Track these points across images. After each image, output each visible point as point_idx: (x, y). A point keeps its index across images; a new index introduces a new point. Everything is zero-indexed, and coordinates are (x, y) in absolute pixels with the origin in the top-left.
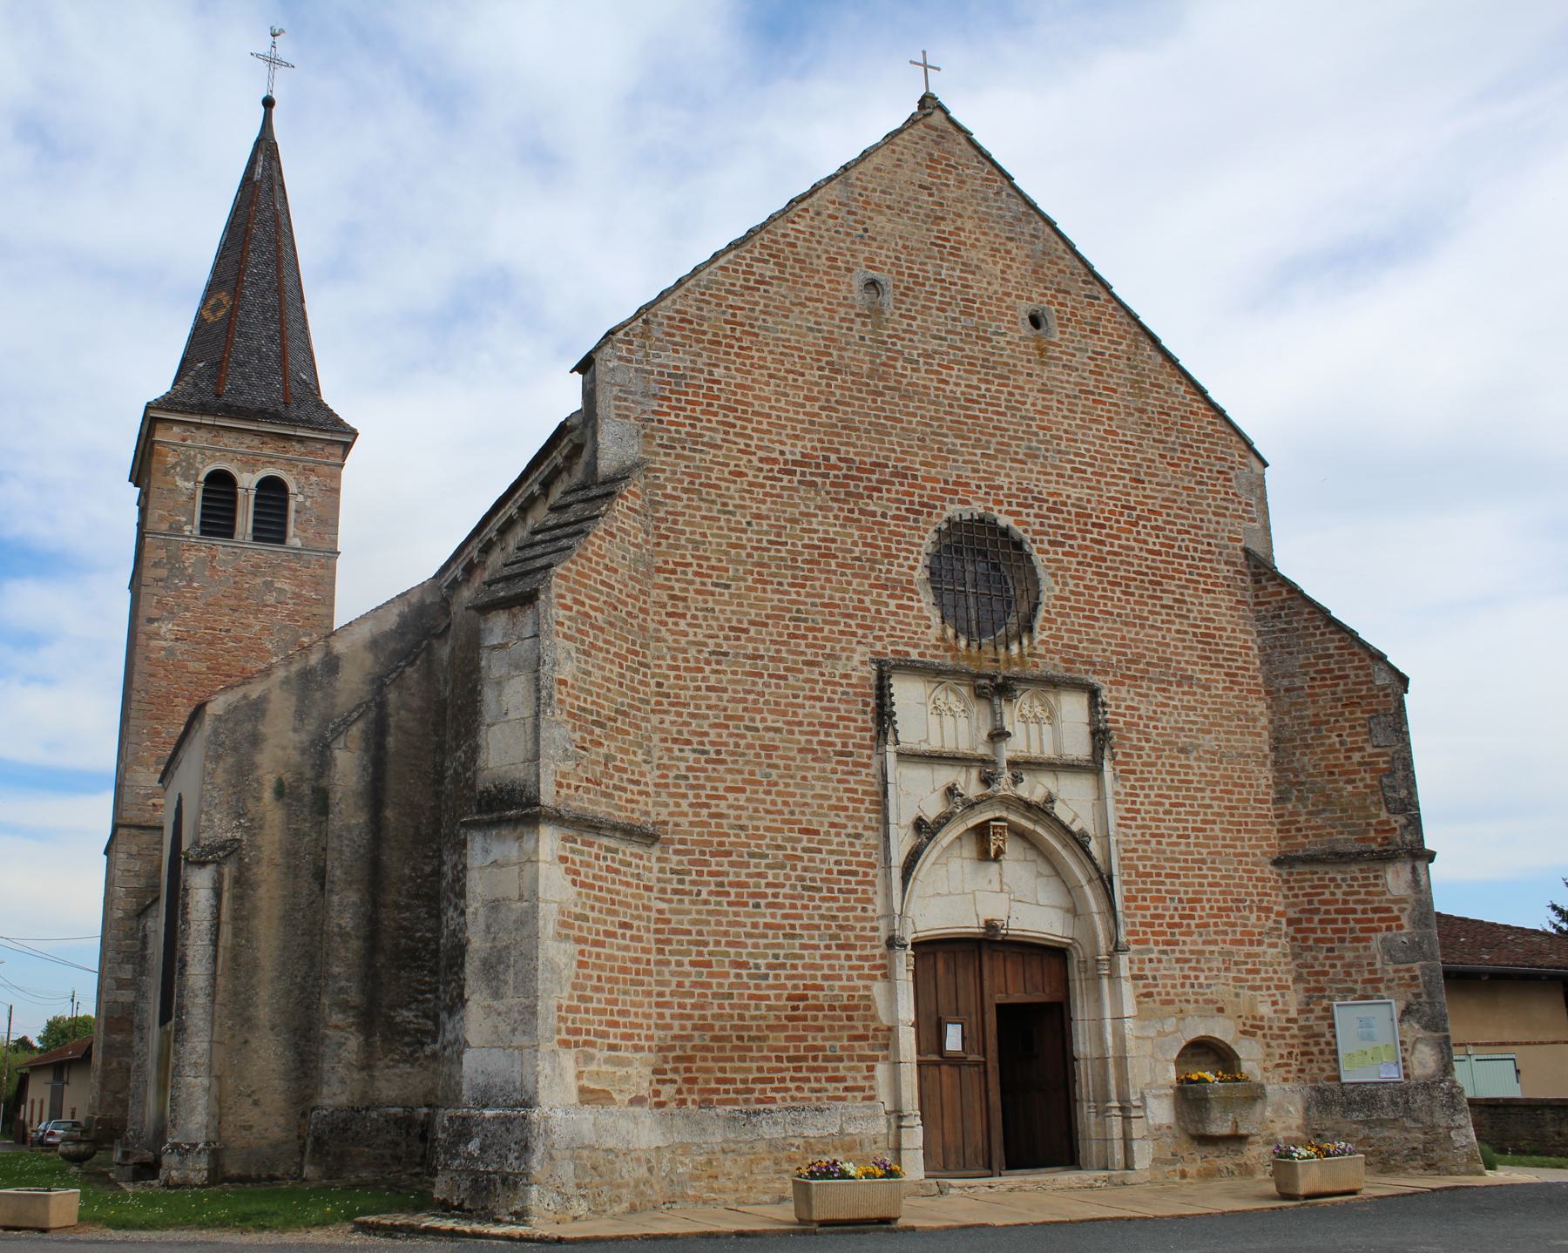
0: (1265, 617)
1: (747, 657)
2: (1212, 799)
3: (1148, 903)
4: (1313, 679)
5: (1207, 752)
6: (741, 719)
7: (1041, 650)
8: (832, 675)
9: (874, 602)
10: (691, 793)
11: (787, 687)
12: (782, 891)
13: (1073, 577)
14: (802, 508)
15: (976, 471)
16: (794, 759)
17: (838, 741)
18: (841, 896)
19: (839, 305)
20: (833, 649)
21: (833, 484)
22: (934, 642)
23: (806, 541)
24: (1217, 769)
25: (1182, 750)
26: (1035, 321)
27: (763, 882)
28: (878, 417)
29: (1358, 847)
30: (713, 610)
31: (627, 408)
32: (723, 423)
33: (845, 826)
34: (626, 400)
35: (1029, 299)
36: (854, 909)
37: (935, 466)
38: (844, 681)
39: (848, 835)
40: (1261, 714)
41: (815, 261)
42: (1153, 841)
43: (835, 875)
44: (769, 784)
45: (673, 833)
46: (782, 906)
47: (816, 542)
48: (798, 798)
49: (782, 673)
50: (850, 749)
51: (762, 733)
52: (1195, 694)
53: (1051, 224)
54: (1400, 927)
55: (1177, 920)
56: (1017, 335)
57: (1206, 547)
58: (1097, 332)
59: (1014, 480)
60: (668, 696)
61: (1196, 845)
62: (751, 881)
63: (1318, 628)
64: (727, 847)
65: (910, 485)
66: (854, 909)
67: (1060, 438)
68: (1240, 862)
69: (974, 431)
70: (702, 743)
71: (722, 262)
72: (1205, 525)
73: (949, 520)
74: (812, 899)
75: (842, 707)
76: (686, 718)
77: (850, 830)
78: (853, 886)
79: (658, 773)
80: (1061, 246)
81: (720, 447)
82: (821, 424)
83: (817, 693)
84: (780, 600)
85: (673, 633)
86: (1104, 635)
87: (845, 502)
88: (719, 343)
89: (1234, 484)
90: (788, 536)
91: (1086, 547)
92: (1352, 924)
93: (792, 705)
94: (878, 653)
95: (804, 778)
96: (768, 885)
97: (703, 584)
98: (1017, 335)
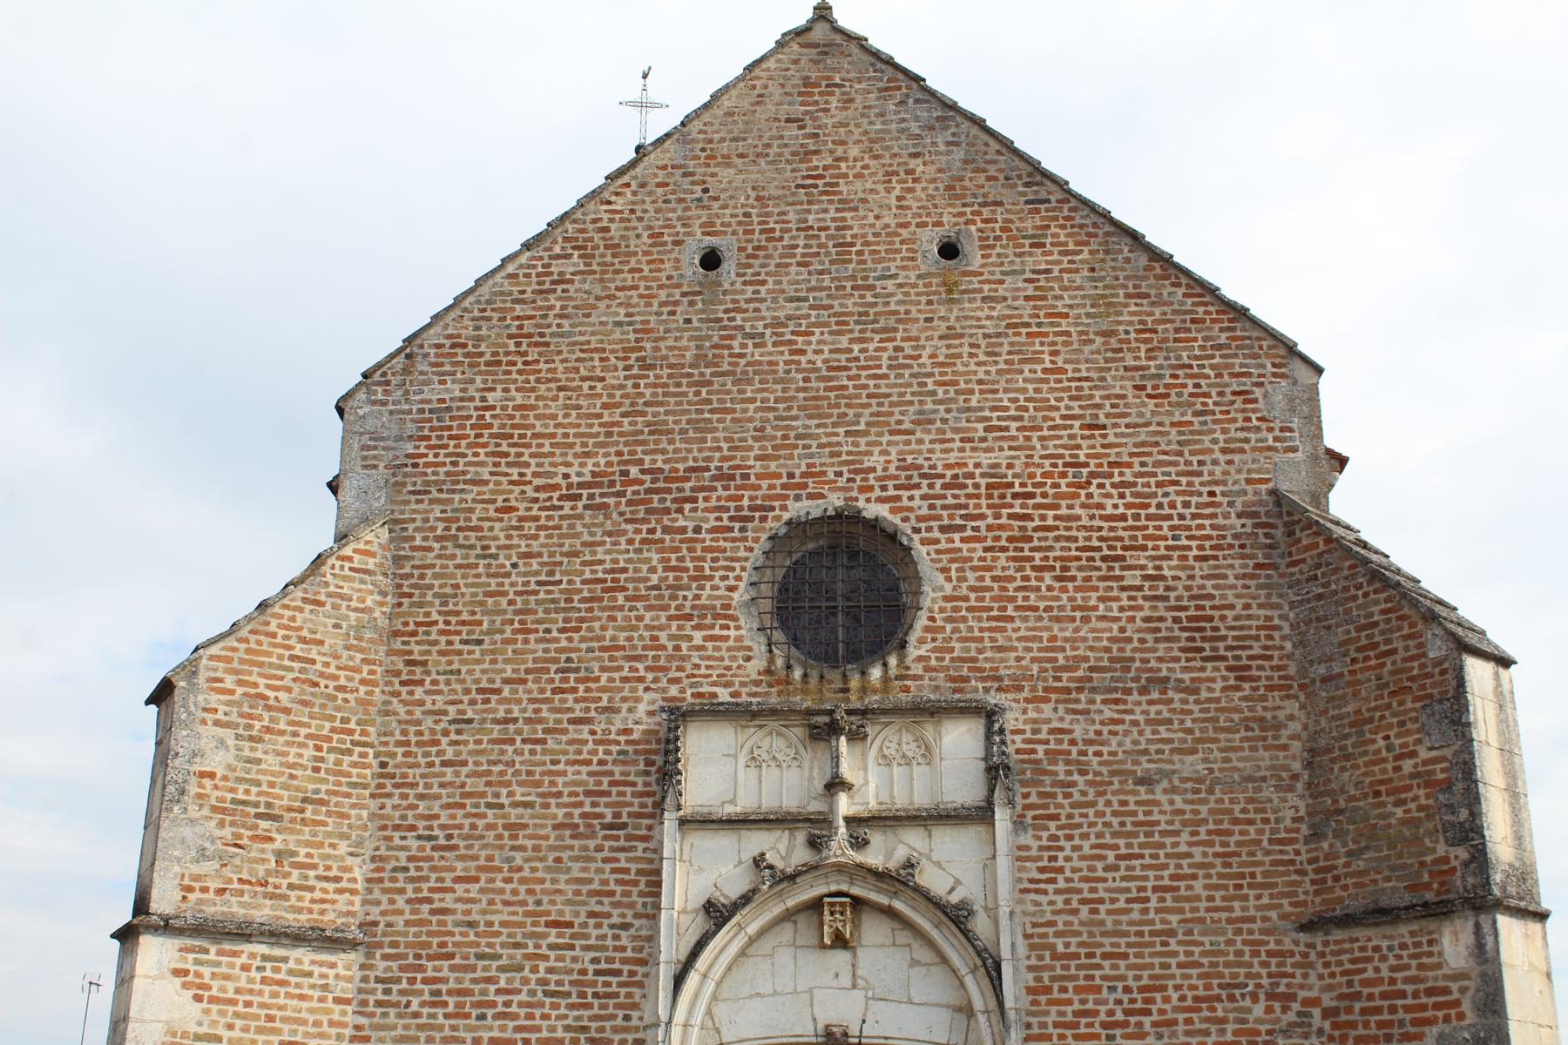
0: (1298, 582)
1: (496, 721)
2: (1191, 844)
3: (1070, 995)
4: (1354, 660)
5: (1184, 780)
6: (483, 795)
7: (917, 669)
8: (607, 732)
9: (671, 637)
10: (410, 887)
11: (544, 752)
12: (516, 998)
13: (974, 569)
14: (586, 537)
15: (832, 455)
16: (546, 838)
17: (608, 812)
18: (596, 1002)
19: (660, 287)
20: (610, 700)
21: (630, 503)
22: (754, 676)
23: (588, 575)
24: (1203, 802)
25: (1141, 781)
26: (949, 251)
27: (492, 988)
28: (701, 412)
29: (1407, 899)
30: (459, 672)
31: (375, 457)
32: (493, 454)
33: (609, 915)
34: (375, 448)
35: (939, 224)
36: (613, 1017)
37: (777, 458)
38: (622, 738)
39: (612, 926)
40: (1291, 717)
41: (632, 243)
42: (1084, 909)
43: (590, 976)
44: (511, 870)
45: (384, 934)
46: (515, 1016)
47: (600, 575)
48: (548, 885)
49: (540, 735)
50: (625, 819)
51: (507, 810)
52: (1171, 701)
53: (979, 123)
54: (1461, 1016)
55: (1119, 1016)
56: (913, 275)
57: (1205, 499)
58: (1043, 245)
59: (893, 456)
60: (393, 776)
61: (1158, 911)
62: (476, 988)
63: (1360, 587)
64: (450, 949)
65: (737, 488)
66: (613, 1017)
67: (972, 392)
68: (1238, 932)
69: (838, 406)
70: (430, 828)
71: (510, 269)
72: (1205, 469)
73: (789, 523)
74: (555, 1006)
75: (617, 769)
76: (412, 800)
77: (615, 920)
78: (614, 989)
79: (373, 866)
80: (995, 146)
81: (486, 483)
82: (621, 434)
83: (585, 756)
84: (546, 651)
85: (405, 703)
86: (1020, 639)
87: (644, 521)
88: (499, 363)
89: (1261, 405)
90: (563, 573)
91: (1001, 527)
92: (1401, 1014)
93: (550, 773)
94: (674, 699)
95: (558, 860)
96: (498, 992)
97: (450, 643)
98: (913, 275)
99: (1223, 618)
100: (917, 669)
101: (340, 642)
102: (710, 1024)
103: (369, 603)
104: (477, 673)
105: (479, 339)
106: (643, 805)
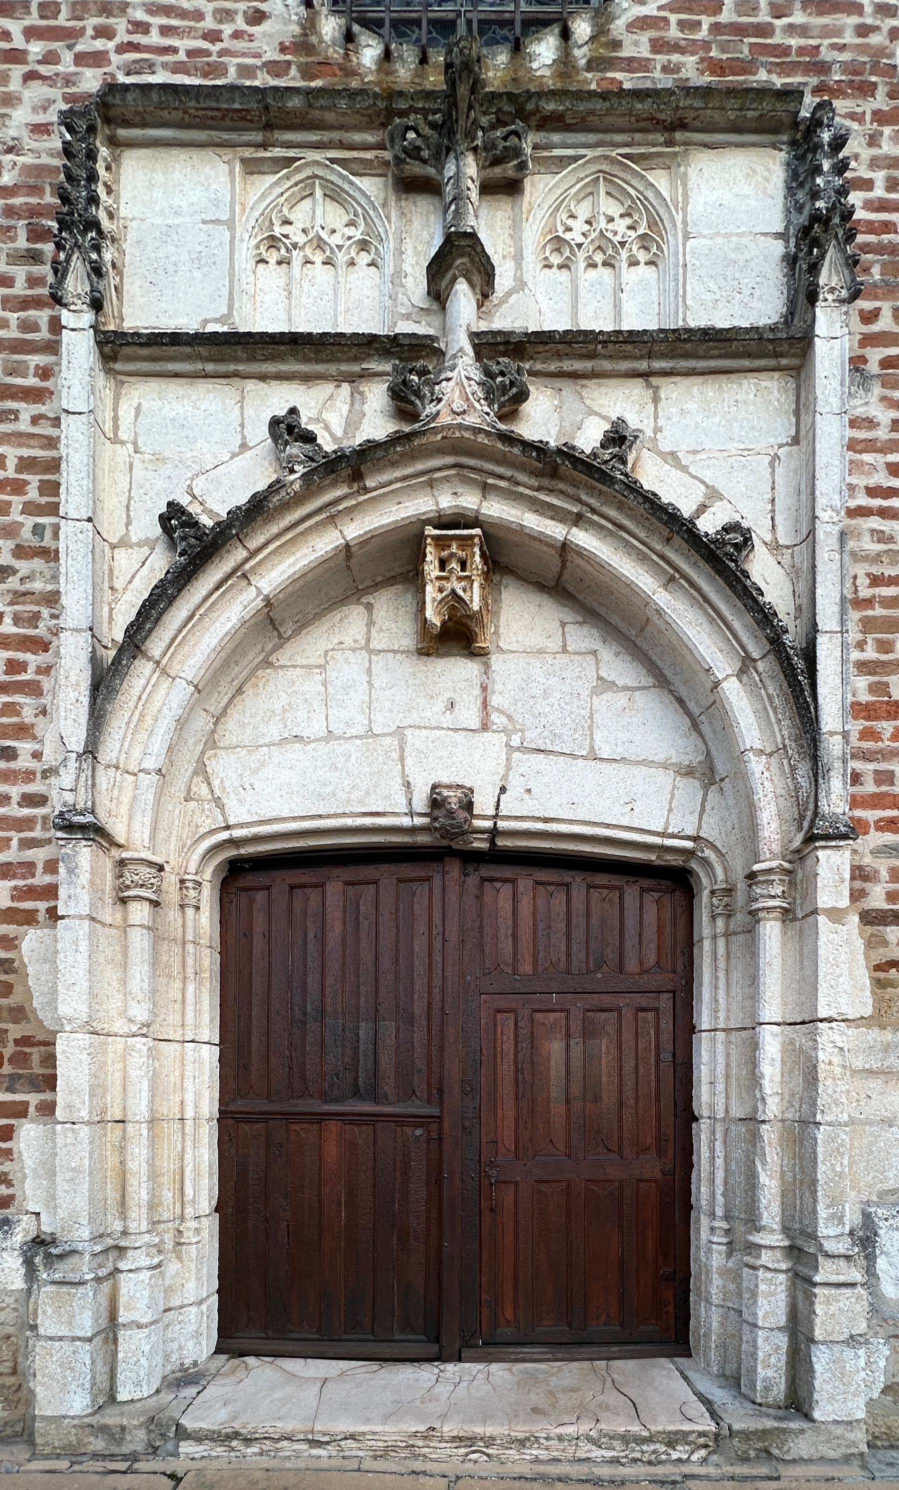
102: (204, 791)
106: (28, 326)
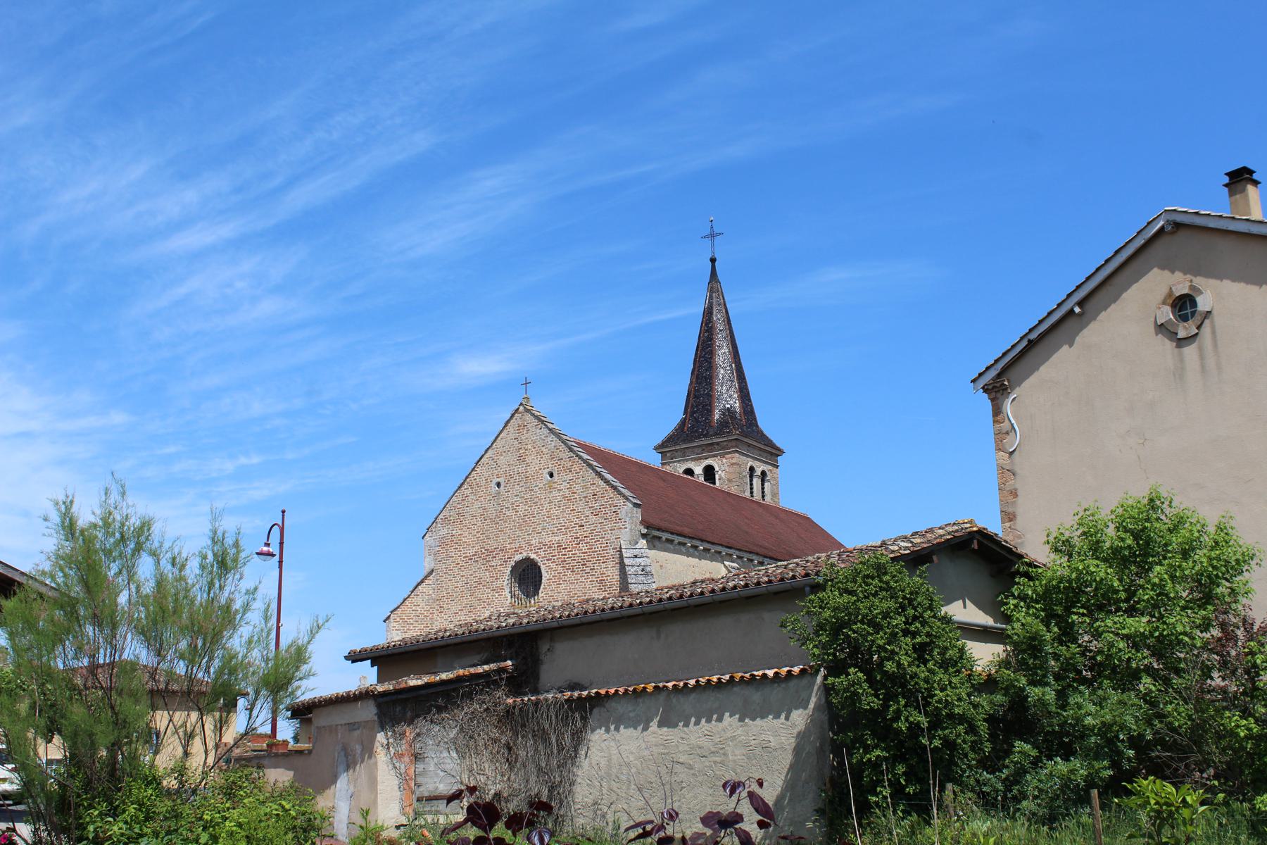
26: (551, 475)
35: (548, 468)
67: (554, 519)
81: (453, 557)
87: (486, 564)
91: (560, 558)
99: (607, 580)
100: (541, 600)
101: (424, 604)
103: (430, 593)
104: (454, 609)
105: (450, 516)
